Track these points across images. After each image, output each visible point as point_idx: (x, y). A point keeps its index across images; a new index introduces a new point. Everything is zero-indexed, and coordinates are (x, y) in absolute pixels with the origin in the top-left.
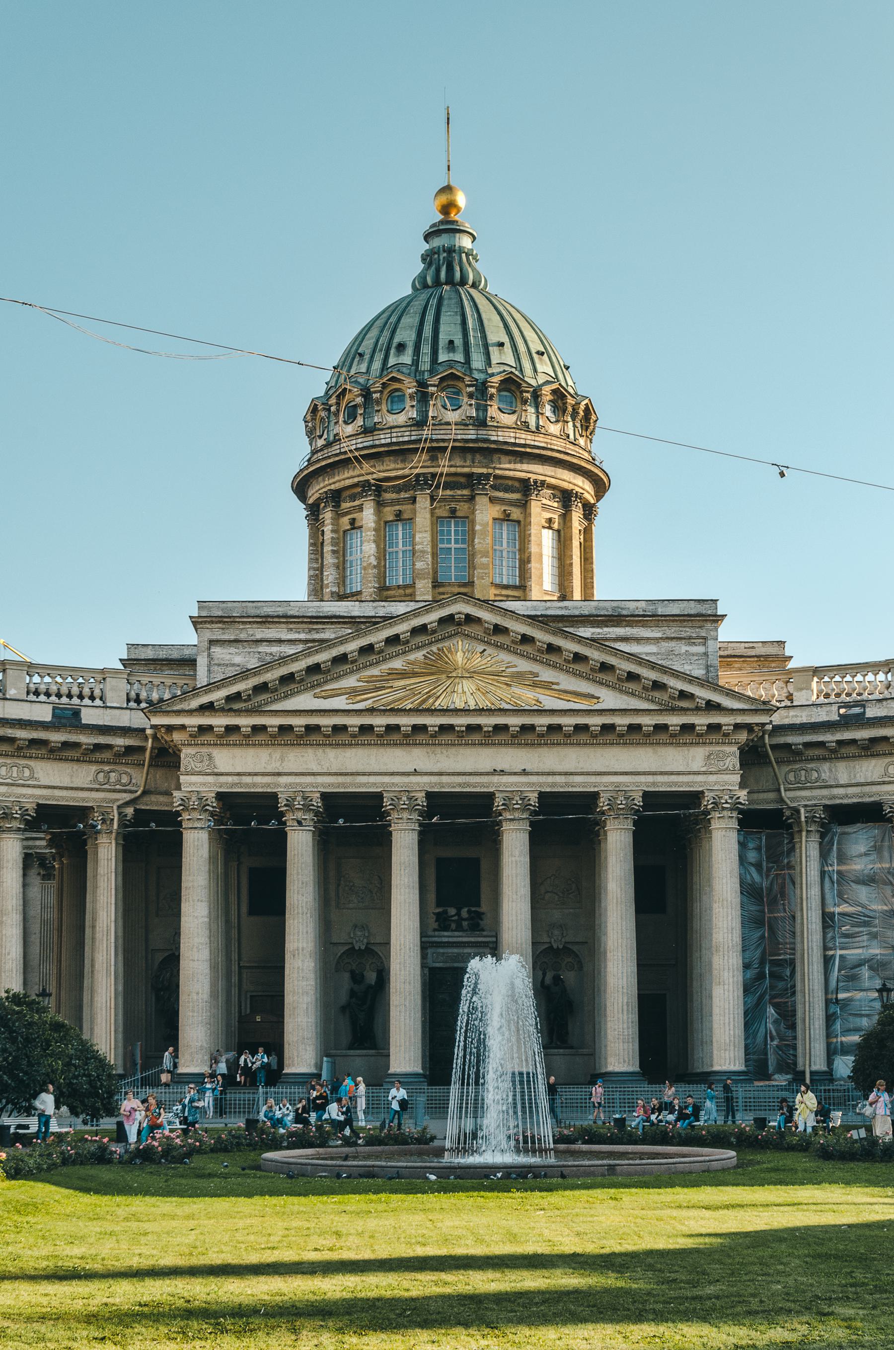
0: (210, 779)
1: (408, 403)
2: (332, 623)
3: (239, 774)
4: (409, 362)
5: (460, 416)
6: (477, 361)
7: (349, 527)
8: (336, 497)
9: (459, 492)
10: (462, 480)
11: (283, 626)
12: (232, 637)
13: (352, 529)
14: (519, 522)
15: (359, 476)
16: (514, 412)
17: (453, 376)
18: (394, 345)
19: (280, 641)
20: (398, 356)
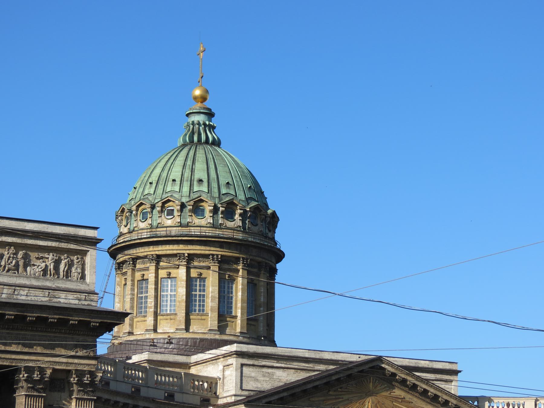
1: (208, 214)
5: (235, 224)
7: (166, 276)
8: (158, 258)
13: (169, 278)
14: (256, 285)
16: (257, 225)
18: (196, 180)
20: (199, 186)
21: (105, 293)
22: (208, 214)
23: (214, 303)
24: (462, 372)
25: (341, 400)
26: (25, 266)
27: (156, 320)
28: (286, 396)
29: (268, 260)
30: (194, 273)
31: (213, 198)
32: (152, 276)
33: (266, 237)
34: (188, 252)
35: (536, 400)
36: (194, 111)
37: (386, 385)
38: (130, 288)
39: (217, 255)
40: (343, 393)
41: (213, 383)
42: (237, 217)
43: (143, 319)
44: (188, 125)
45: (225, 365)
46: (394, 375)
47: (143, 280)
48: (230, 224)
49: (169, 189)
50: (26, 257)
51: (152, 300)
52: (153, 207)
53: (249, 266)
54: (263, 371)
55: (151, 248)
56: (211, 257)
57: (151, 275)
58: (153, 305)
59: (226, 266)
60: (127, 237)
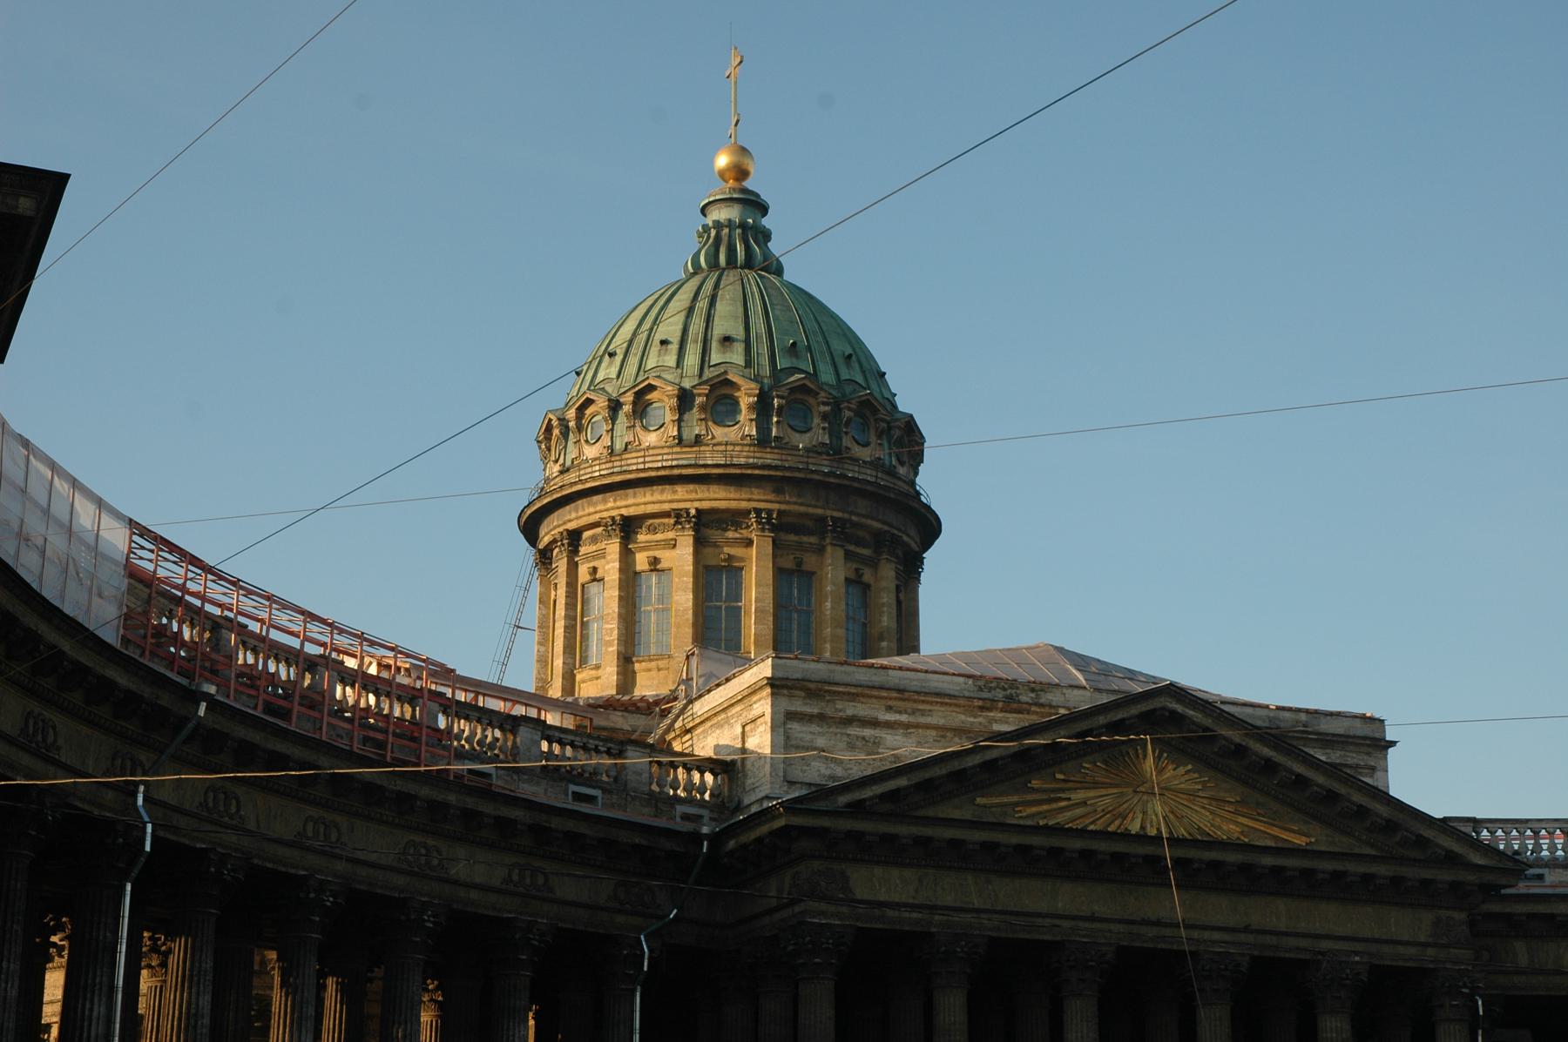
0: (844, 909)
1: (745, 415)
2: (942, 704)
3: (881, 904)
6: (827, 376)
8: (628, 527)
9: (805, 539)
10: (810, 523)
11: (883, 702)
12: (813, 708)
14: (866, 587)
15: (671, 501)
16: (866, 445)
17: (802, 388)
18: (715, 338)
19: (874, 723)
20: (724, 353)
21: (519, 630)
22: (745, 415)
23: (762, 627)
24: (1398, 744)
25: (1063, 804)
28: (905, 788)
29: (900, 530)
31: (757, 379)
32: (613, 568)
33: (891, 472)
34: (697, 504)
36: (717, 197)
37: (1190, 767)
38: (564, 602)
39: (769, 512)
40: (1070, 785)
42: (816, 421)
43: (593, 673)
44: (706, 229)
45: (742, 720)
47: (594, 580)
51: (612, 626)
52: (615, 406)
54: (849, 732)
56: (753, 515)
57: (612, 564)
58: (616, 637)
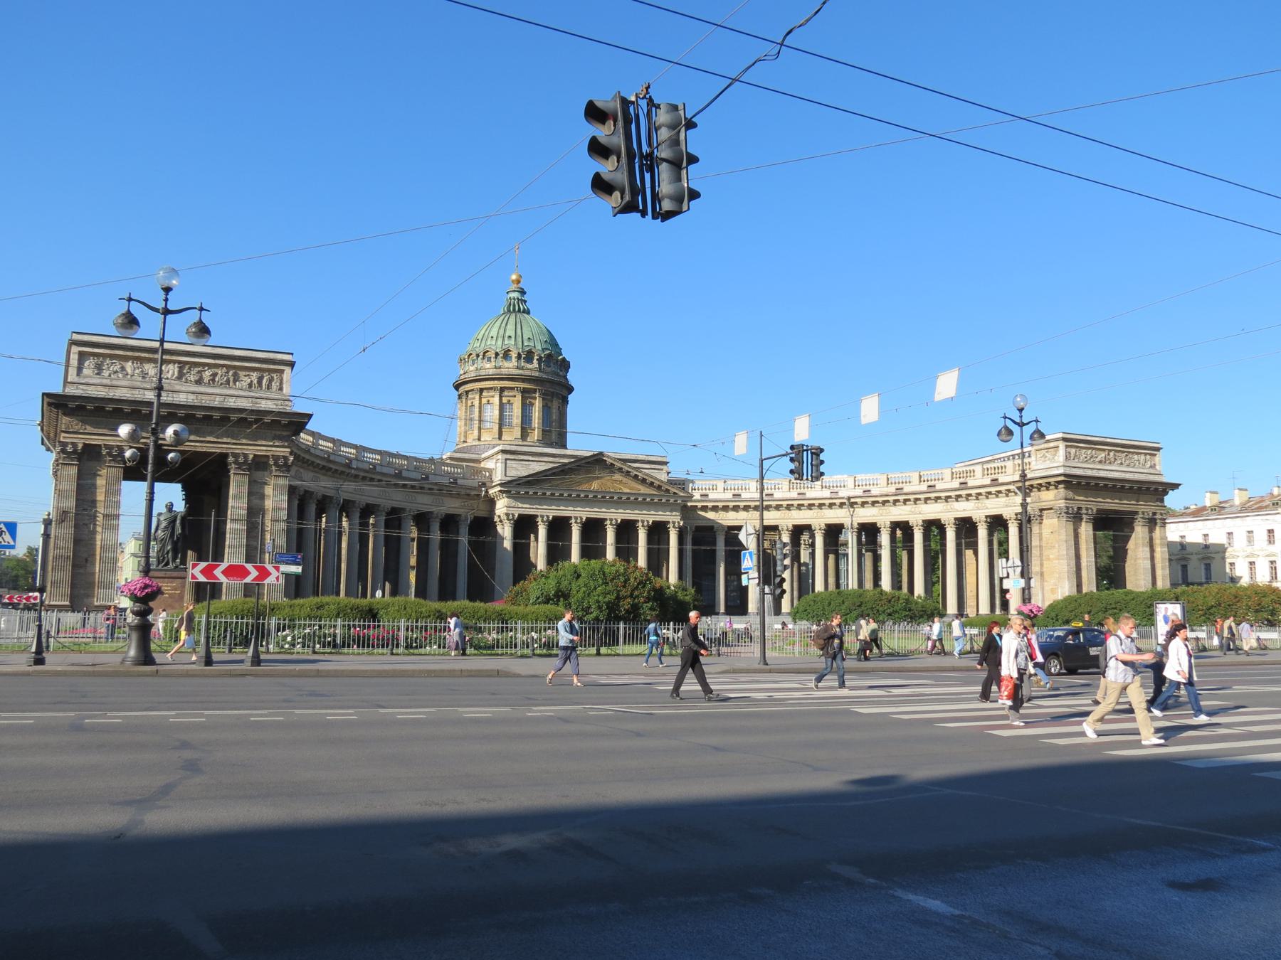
4: (513, 343)
8: (481, 390)
14: (550, 408)
16: (550, 367)
19: (529, 461)
22: (514, 359)
26: (235, 381)
27: (480, 432)
30: (505, 400)
33: (558, 375)
35: (725, 482)
41: (490, 471)
42: (535, 361)
46: (612, 465)
48: (530, 366)
49: (488, 343)
50: (235, 375)
52: (478, 356)
53: (543, 394)
55: (477, 384)
59: (527, 395)
60: (463, 377)
